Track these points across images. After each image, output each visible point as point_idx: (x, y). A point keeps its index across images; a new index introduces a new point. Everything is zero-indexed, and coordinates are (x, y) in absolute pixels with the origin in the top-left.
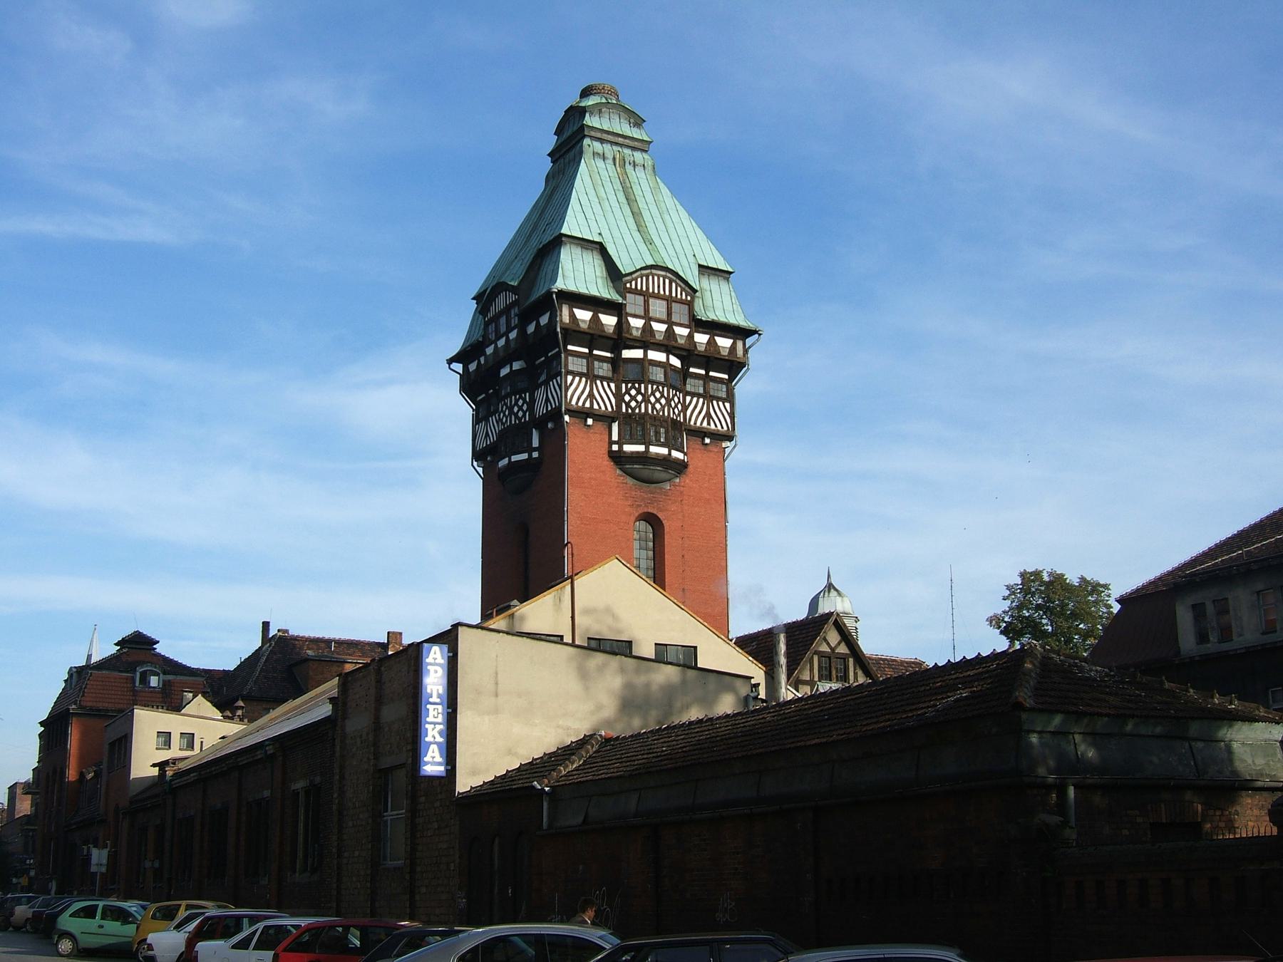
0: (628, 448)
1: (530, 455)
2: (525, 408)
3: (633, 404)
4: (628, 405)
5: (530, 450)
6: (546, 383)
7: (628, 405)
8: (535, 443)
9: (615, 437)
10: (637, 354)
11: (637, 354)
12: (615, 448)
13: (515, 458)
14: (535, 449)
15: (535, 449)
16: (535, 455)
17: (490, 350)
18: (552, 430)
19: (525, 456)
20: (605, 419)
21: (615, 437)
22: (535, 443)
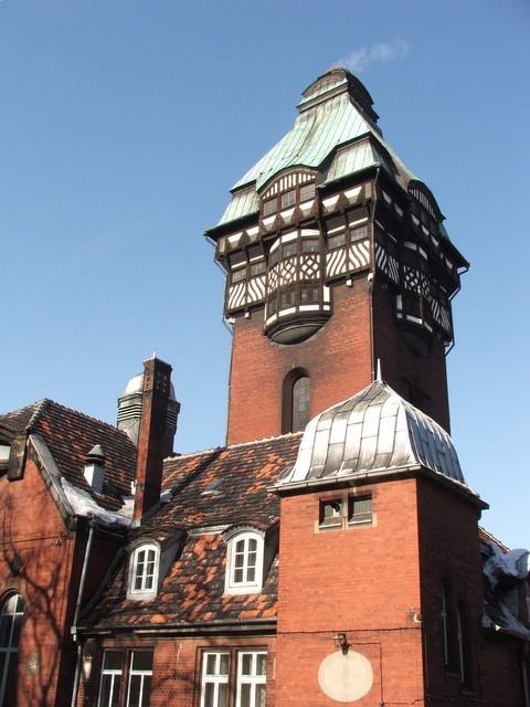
0: (410, 318)
1: (321, 307)
2: (316, 267)
3: (413, 284)
4: (409, 284)
5: (322, 303)
6: (347, 246)
7: (409, 284)
8: (327, 298)
9: (400, 306)
10: (414, 247)
11: (414, 247)
12: (400, 316)
13: (303, 308)
14: (327, 303)
15: (327, 303)
16: (327, 308)
17: (269, 222)
18: (350, 287)
19: (316, 308)
20: (396, 289)
21: (400, 306)
22: (327, 298)
